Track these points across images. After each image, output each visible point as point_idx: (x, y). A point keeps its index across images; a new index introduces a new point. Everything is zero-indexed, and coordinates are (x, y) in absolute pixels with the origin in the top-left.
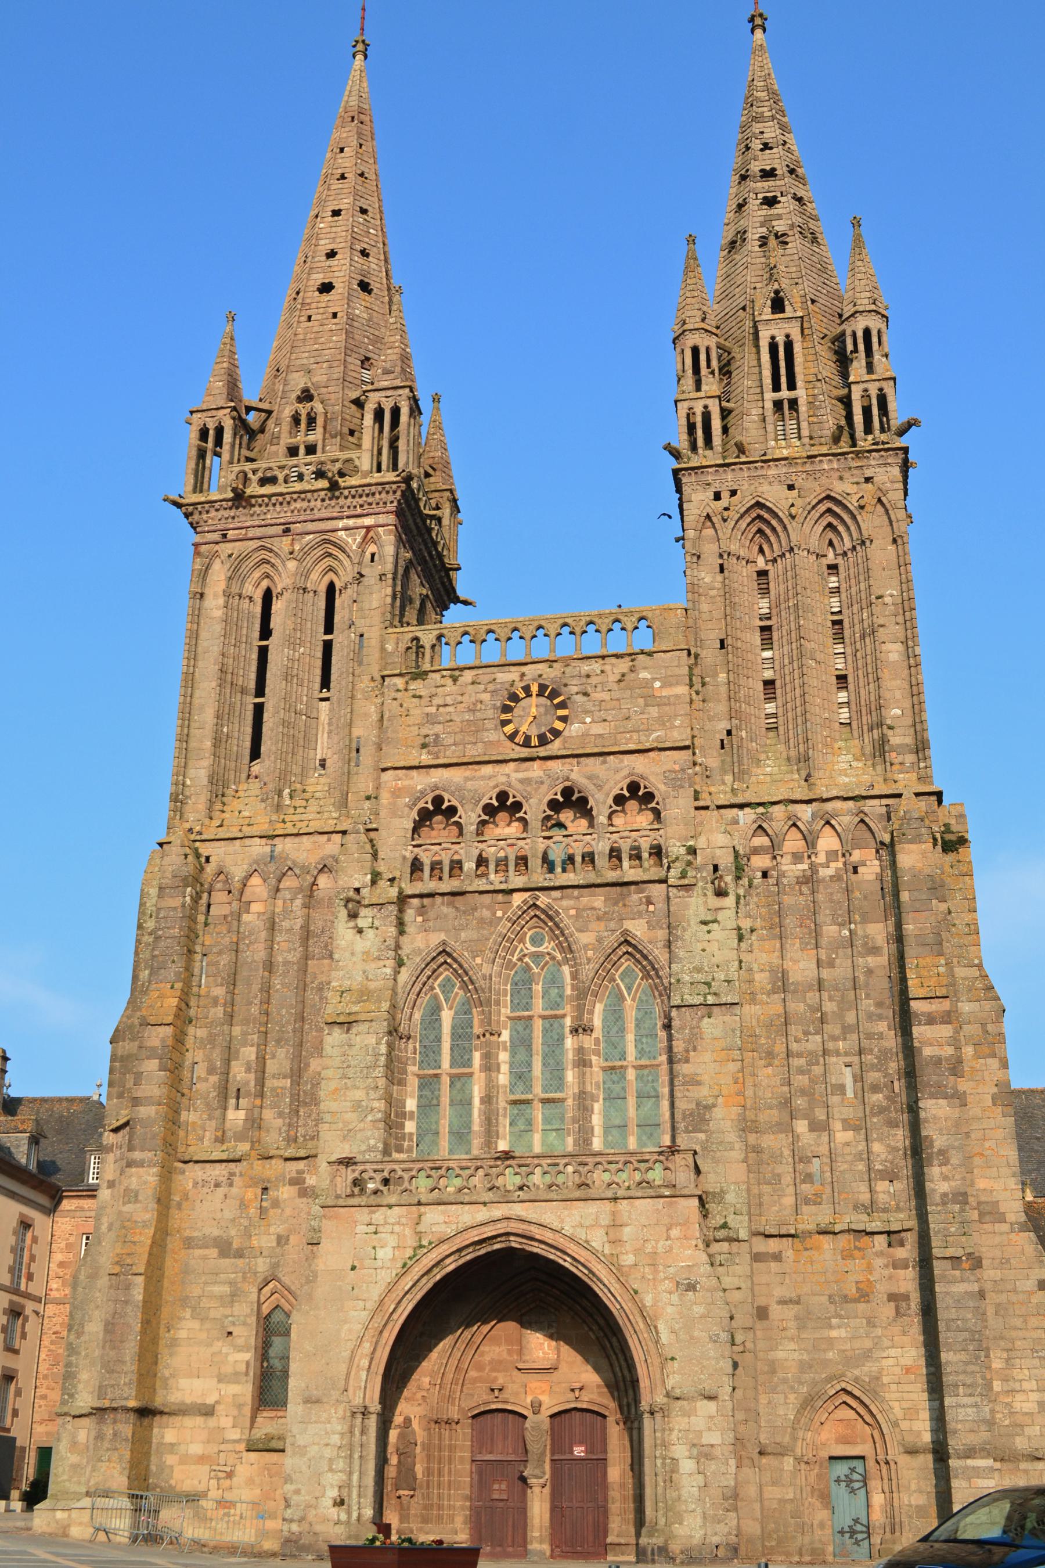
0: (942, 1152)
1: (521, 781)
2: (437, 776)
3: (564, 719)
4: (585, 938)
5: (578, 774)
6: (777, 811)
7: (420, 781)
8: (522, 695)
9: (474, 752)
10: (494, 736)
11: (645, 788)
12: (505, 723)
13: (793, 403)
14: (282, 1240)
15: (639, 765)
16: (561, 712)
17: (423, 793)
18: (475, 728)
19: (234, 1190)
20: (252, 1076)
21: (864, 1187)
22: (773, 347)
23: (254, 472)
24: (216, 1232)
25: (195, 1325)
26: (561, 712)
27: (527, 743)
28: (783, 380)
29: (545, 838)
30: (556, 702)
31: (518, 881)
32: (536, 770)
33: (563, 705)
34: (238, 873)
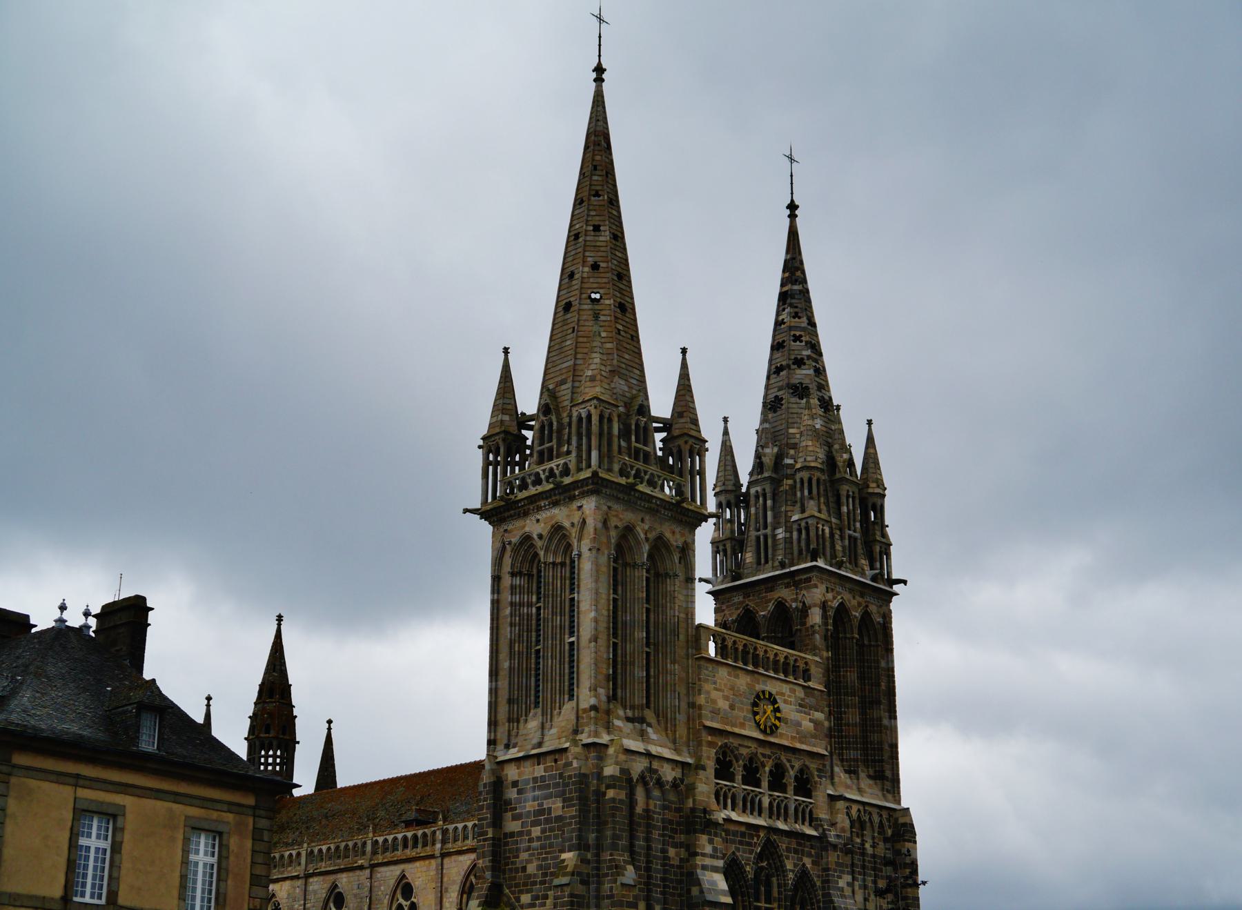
3: (779, 719)
4: (789, 865)
6: (855, 808)
16: (778, 715)
17: (721, 747)
26: (778, 715)
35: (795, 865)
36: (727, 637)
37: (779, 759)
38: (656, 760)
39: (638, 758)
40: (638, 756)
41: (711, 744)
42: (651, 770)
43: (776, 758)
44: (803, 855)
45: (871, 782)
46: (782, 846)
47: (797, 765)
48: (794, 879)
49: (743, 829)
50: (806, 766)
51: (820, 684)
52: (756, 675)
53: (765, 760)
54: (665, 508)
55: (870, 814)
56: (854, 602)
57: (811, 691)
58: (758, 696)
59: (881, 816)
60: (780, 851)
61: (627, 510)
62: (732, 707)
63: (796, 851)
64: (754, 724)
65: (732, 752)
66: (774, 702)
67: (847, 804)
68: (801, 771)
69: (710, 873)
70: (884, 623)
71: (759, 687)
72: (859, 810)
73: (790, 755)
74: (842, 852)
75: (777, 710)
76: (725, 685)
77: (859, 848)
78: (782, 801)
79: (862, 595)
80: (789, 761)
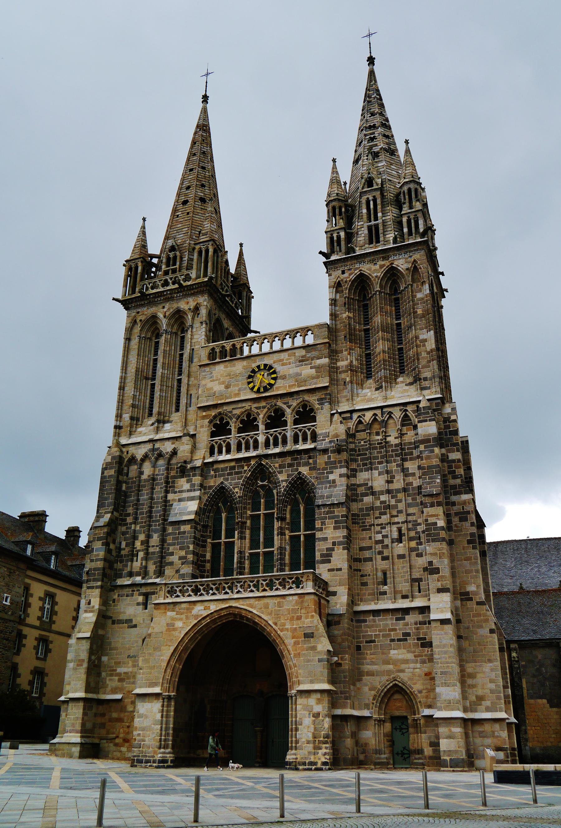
1: (256, 408)
3: (275, 379)
4: (282, 477)
8: (257, 370)
11: (310, 406)
12: (249, 383)
15: (306, 397)
16: (273, 376)
17: (215, 417)
23: (149, 284)
26: (273, 376)
27: (258, 391)
28: (372, 216)
29: (266, 433)
30: (271, 371)
33: (274, 372)
35: (289, 476)
36: (225, 345)
37: (276, 405)
38: (159, 442)
39: (142, 446)
40: (143, 444)
41: (204, 417)
42: (153, 450)
43: (271, 406)
44: (299, 465)
45: (407, 387)
46: (274, 466)
47: (294, 403)
48: (287, 486)
49: (233, 464)
50: (306, 401)
51: (325, 338)
52: (252, 358)
53: (258, 411)
54: (175, 293)
55: (390, 413)
56: (377, 267)
57: (311, 348)
58: (253, 371)
59: (406, 410)
60: (272, 469)
61: (152, 307)
62: (227, 387)
63: (290, 465)
64: (249, 391)
65: (226, 415)
66: (271, 367)
67: (360, 414)
68: (304, 406)
69: (186, 502)
70: (415, 267)
71: (254, 365)
72: (375, 415)
73: (286, 400)
74: (333, 452)
75: (274, 372)
76: (221, 375)
77: (378, 444)
78: (280, 433)
79: (384, 259)
80: (285, 403)
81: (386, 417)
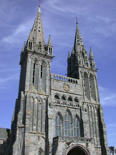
0: (106, 140)
2: (57, 92)
4: (73, 113)
5: (71, 95)
7: (56, 92)
9: (61, 90)
10: (63, 89)
13: (88, 63)
14: (41, 144)
15: (77, 96)
18: (61, 87)
19: (35, 137)
20: (36, 123)
21: (96, 143)
22: (86, 57)
24: (33, 142)
25: (31, 153)
31: (66, 106)
32: (67, 94)
33: (70, 87)
34: (34, 97)
81: (92, 106)
